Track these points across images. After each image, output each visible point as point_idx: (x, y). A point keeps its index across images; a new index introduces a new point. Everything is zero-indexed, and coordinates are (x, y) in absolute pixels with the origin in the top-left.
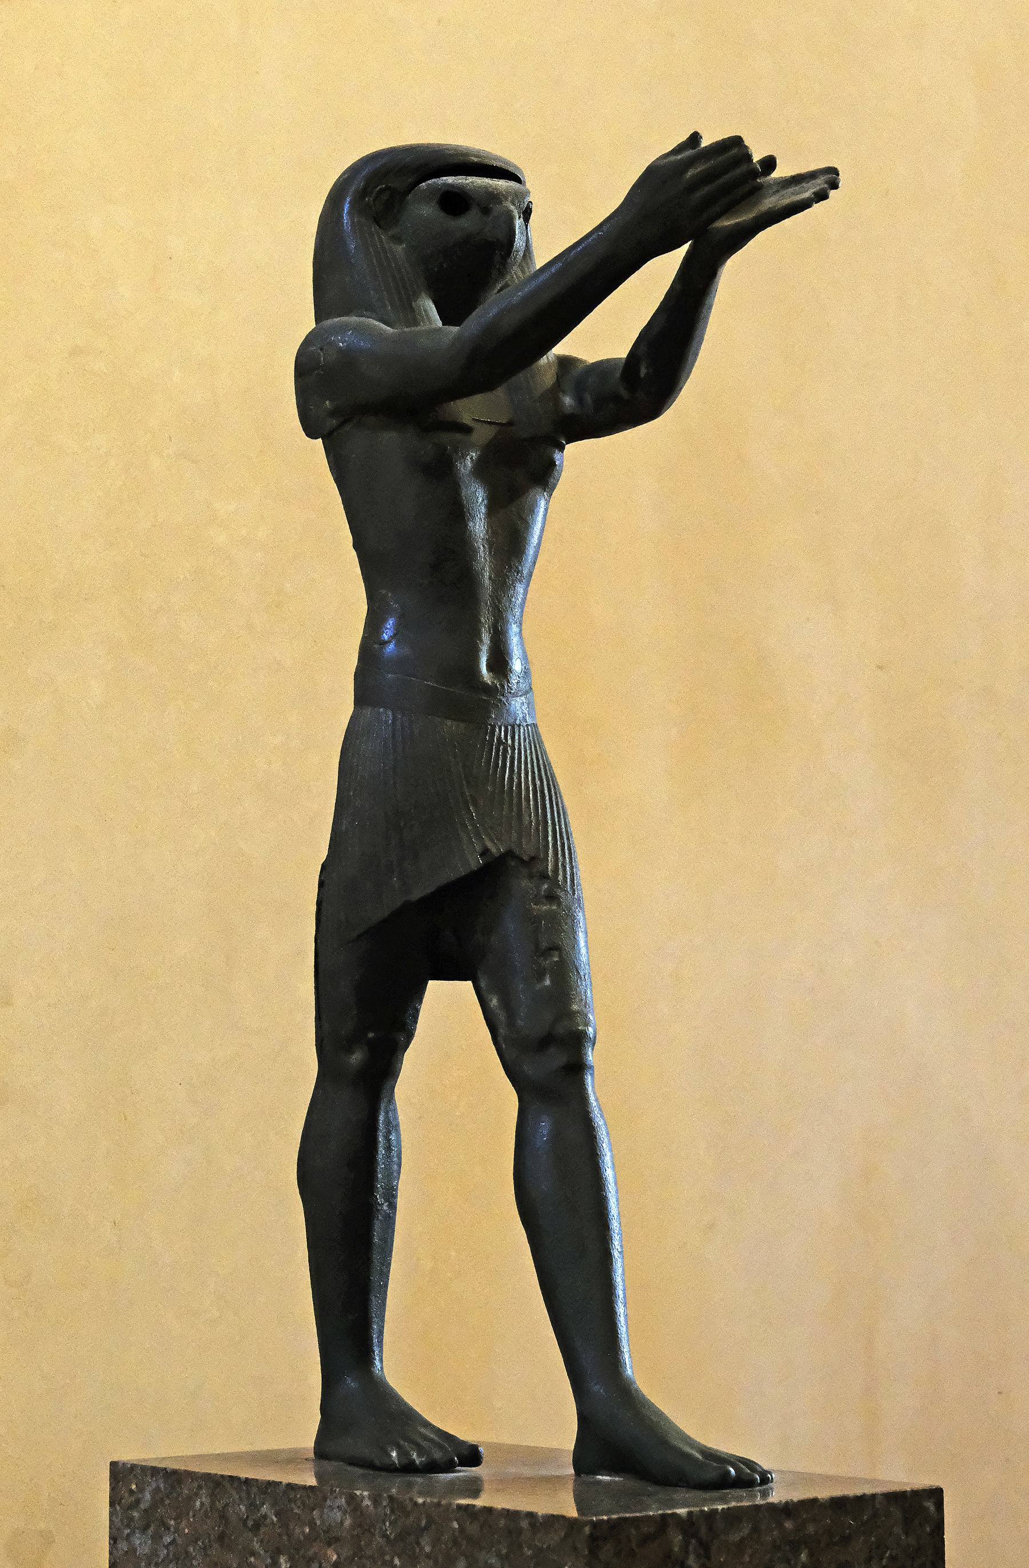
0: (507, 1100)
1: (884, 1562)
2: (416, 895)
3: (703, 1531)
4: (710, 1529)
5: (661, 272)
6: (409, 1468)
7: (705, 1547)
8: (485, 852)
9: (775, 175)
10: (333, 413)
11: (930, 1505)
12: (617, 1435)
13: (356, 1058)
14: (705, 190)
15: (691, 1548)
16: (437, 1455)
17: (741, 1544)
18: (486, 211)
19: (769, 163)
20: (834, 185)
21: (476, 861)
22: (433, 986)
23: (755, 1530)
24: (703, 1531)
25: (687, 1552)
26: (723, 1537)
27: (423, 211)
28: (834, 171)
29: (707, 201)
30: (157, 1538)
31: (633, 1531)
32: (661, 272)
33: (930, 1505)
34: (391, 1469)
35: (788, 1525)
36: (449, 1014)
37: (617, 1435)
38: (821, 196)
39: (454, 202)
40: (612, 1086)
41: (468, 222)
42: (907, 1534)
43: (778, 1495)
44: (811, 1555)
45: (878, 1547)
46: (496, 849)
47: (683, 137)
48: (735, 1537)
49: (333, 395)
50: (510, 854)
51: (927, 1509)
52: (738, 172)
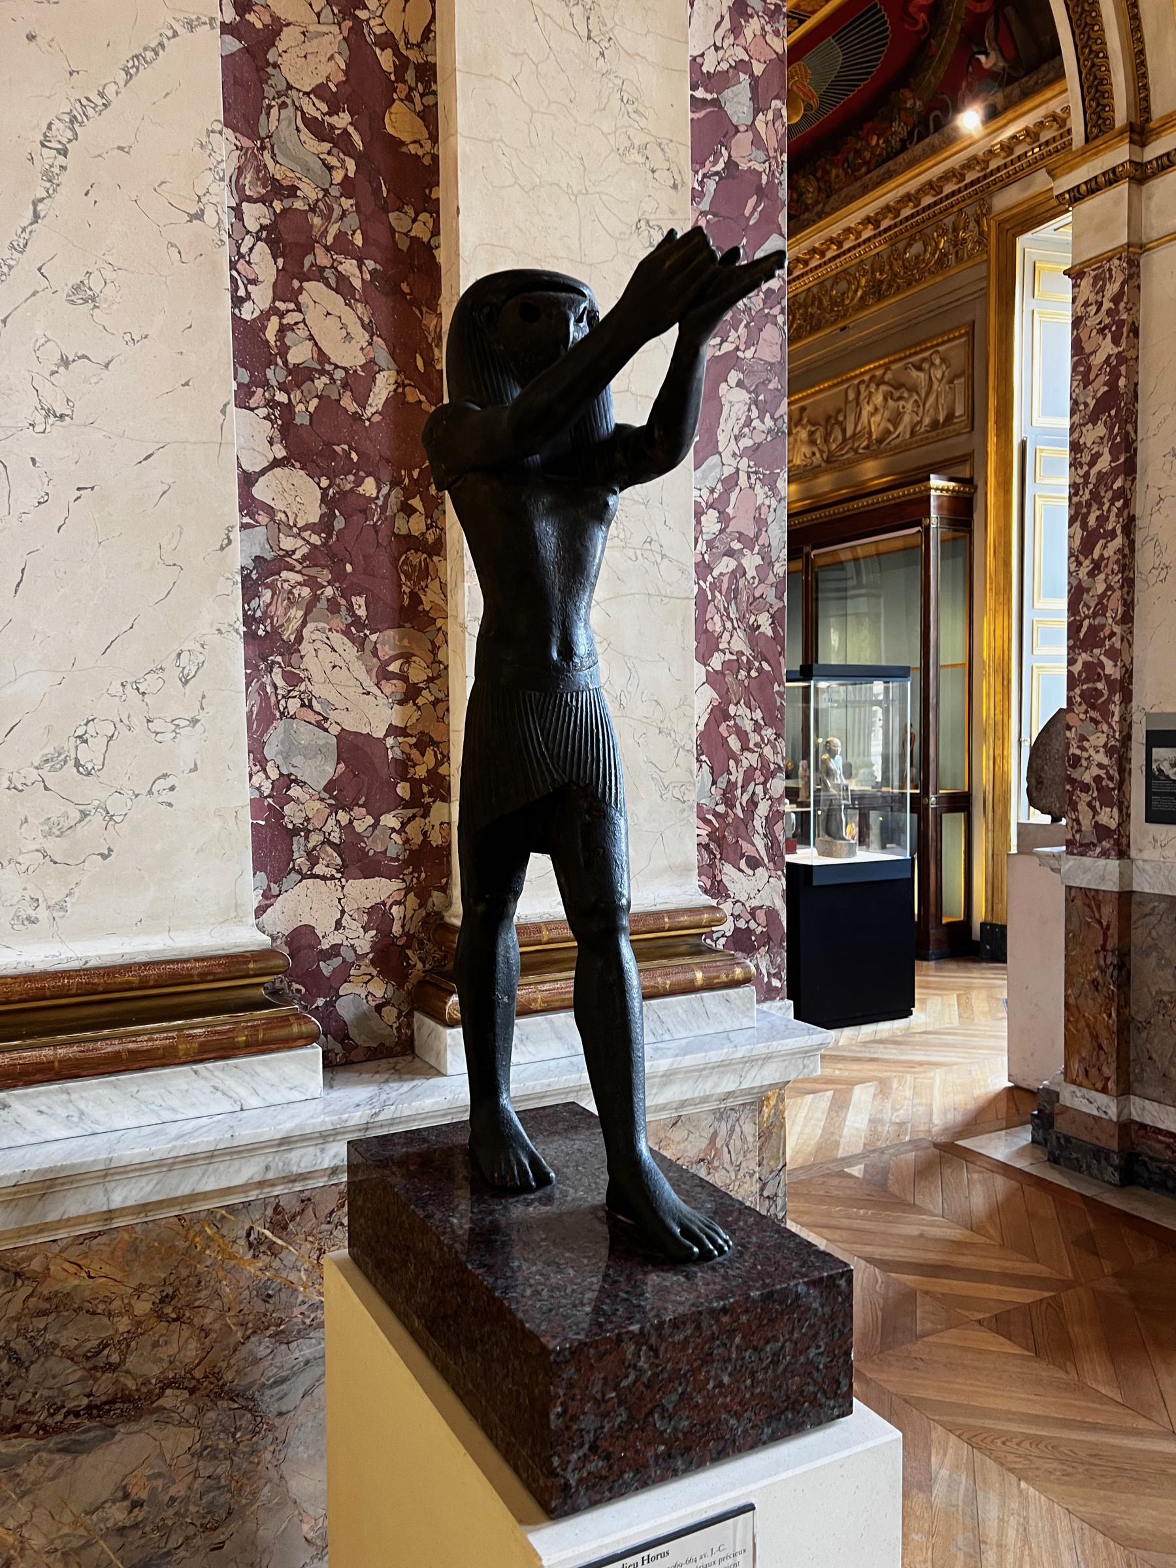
4: (659, 1336)
23: (698, 1327)
24: (653, 1340)
25: (639, 1357)
31: (592, 1351)
33: (842, 1282)
35: (725, 1319)
44: (743, 1337)
45: (799, 1320)
51: (838, 1286)
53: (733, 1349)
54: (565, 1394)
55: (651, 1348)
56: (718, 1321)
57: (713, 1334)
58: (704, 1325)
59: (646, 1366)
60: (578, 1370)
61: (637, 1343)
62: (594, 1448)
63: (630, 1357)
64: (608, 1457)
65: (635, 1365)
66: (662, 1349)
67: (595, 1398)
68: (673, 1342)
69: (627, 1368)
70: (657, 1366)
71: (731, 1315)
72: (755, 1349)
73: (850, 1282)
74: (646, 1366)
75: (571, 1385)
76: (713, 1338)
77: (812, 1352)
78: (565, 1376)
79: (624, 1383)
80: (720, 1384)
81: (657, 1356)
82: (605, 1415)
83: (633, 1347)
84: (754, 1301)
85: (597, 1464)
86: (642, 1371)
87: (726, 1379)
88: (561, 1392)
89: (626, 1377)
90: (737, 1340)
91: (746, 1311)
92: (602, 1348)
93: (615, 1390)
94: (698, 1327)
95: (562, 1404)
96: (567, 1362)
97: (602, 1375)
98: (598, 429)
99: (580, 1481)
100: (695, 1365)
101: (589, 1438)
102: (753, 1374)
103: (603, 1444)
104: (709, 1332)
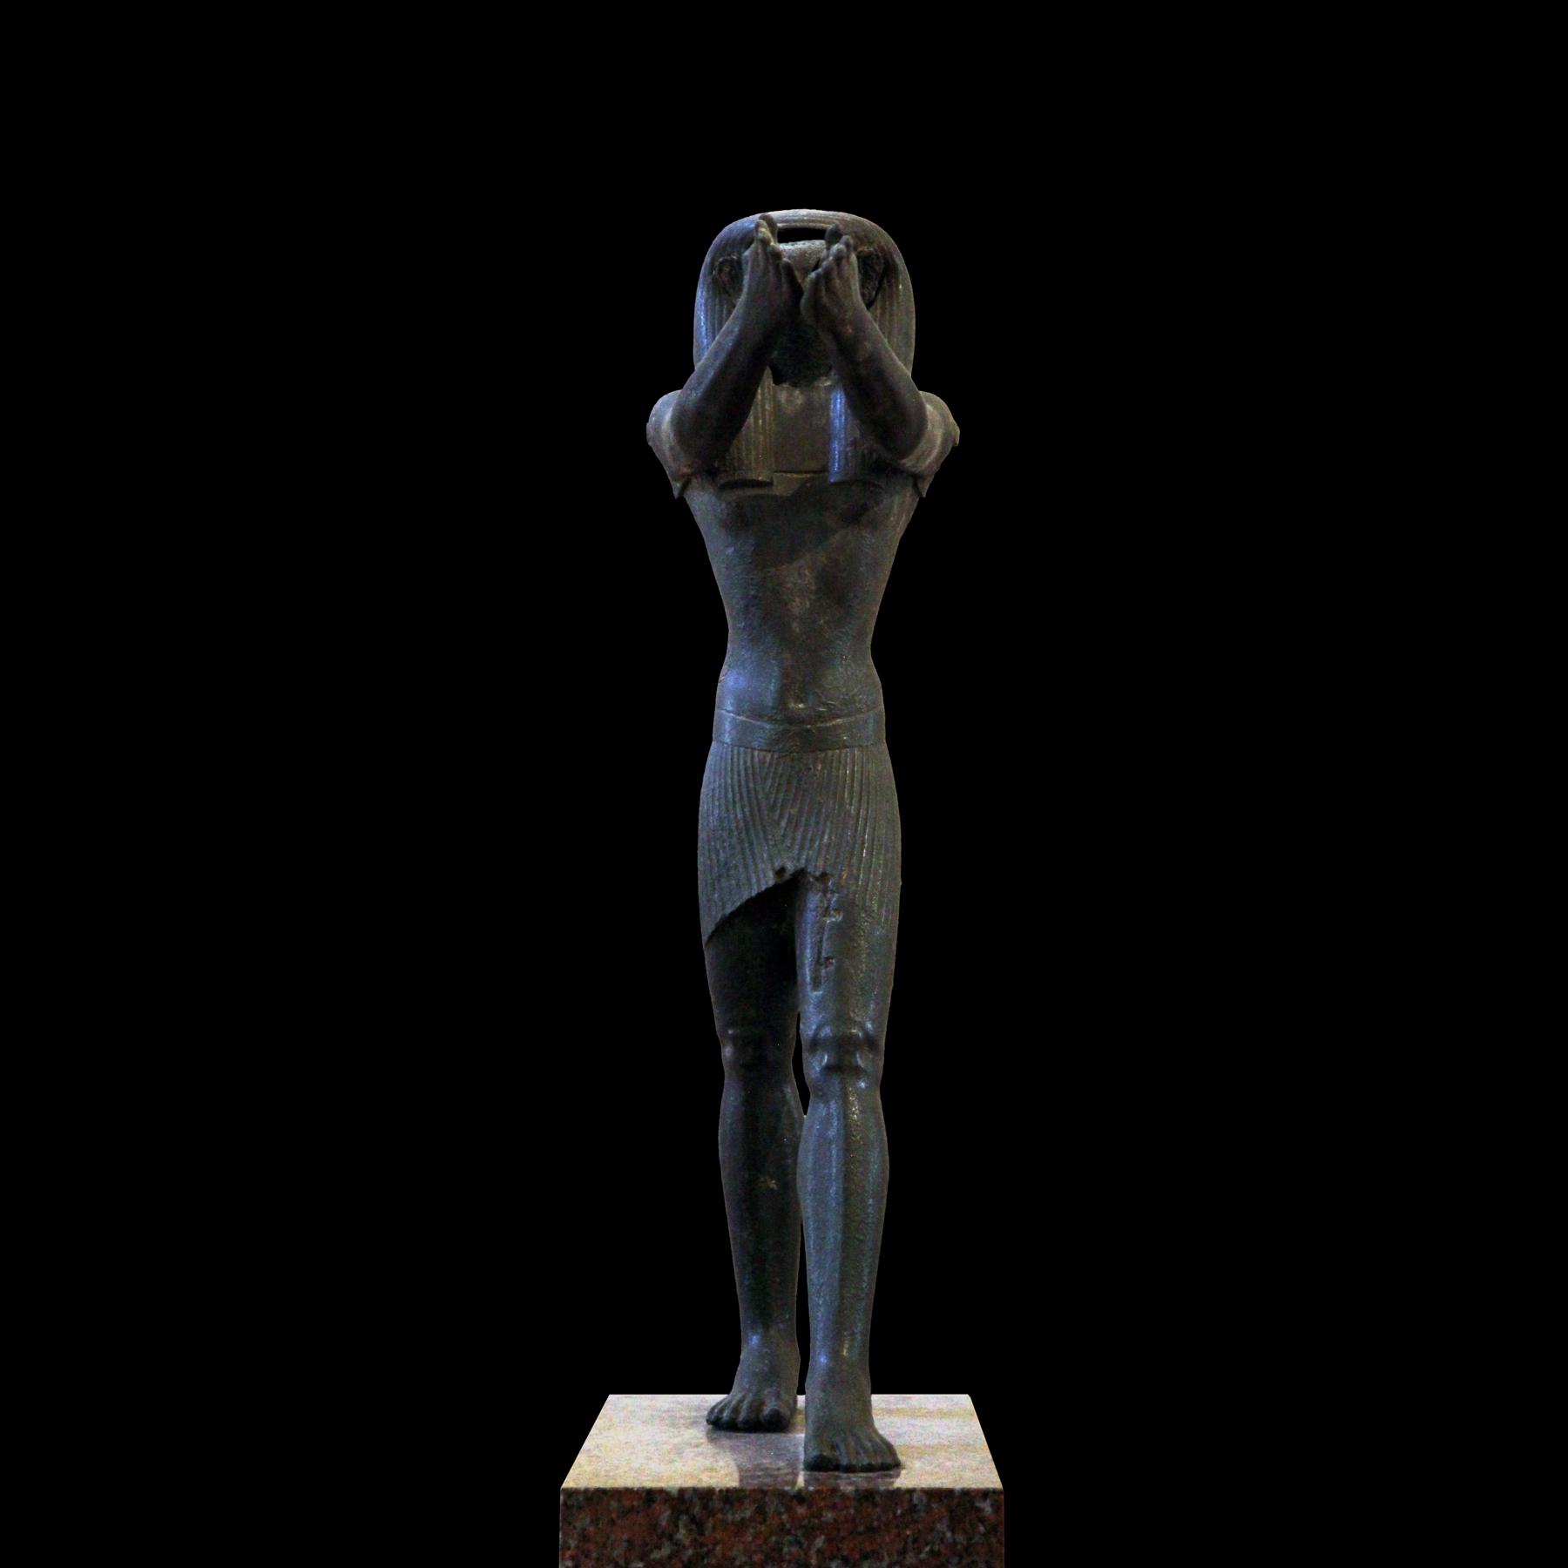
1: (922, 1556)
2: (729, 909)
3: (697, 1510)
4: (705, 1507)
7: (697, 1524)
15: (681, 1524)
17: (741, 1526)
21: (769, 880)
23: (761, 1510)
24: (697, 1510)
26: (719, 1516)
35: (801, 1510)
42: (953, 1531)
43: (903, 1481)
44: (829, 1540)
45: (915, 1541)
48: (733, 1516)
51: (979, 1510)
53: (813, 1552)
54: (577, 1547)
55: (693, 1520)
56: (789, 1509)
57: (783, 1524)
58: (771, 1509)
59: (687, 1542)
60: (595, 1521)
61: (674, 1509)
63: (664, 1523)
65: (670, 1537)
66: (710, 1524)
67: (616, 1563)
68: (723, 1521)
69: (660, 1538)
70: (702, 1545)
71: (810, 1507)
74: (687, 1542)
75: (584, 1537)
76: (782, 1530)
78: (578, 1524)
79: (656, 1555)
81: (702, 1534)
83: (668, 1513)
84: (844, 1496)
86: (678, 1547)
88: (572, 1543)
89: (659, 1547)
90: (820, 1542)
91: (833, 1507)
92: (627, 1503)
93: (642, 1560)
94: (761, 1510)
95: (572, 1558)
96: (580, 1508)
97: (625, 1537)
98: (848, 395)
100: (756, 1558)
104: (775, 1522)
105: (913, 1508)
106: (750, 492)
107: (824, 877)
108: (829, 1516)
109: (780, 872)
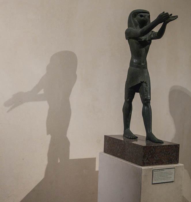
0: (142, 105)
5: (160, 26)
6: (131, 138)
7: (155, 149)
8: (141, 81)
9: (172, 16)
10: (128, 38)
11: (178, 146)
12: (150, 137)
13: (128, 100)
14: (165, 17)
16: (133, 137)
18: (144, 17)
19: (171, 15)
20: (177, 18)
22: (136, 93)
27: (138, 16)
28: (177, 16)
29: (165, 19)
30: (108, 143)
32: (160, 26)
33: (178, 146)
34: (129, 138)
35: (163, 147)
36: (137, 96)
37: (150, 137)
38: (176, 19)
39: (141, 16)
40: (152, 104)
41: (143, 18)
46: (142, 81)
47: (163, 12)
48: (158, 148)
49: (129, 36)
50: (143, 81)
52: (168, 16)
62: (147, 159)
64: (149, 160)
72: (167, 152)
73: (179, 146)
77: (174, 154)
80: (162, 155)
82: (149, 155)
85: (147, 161)
87: (163, 155)
94: (160, 148)
99: (146, 162)
101: (147, 158)
102: (166, 155)
103: (149, 159)
105: (172, 146)
106: (141, 40)
107: (145, 82)
108: (166, 148)
109: (141, 81)
